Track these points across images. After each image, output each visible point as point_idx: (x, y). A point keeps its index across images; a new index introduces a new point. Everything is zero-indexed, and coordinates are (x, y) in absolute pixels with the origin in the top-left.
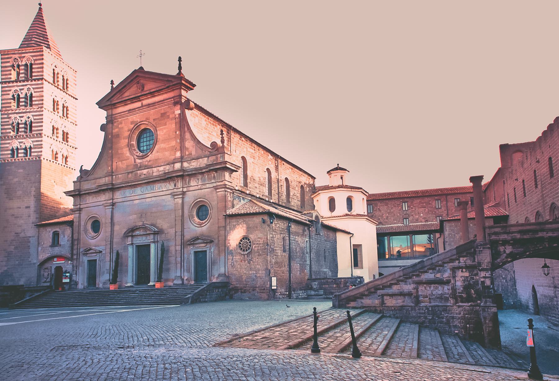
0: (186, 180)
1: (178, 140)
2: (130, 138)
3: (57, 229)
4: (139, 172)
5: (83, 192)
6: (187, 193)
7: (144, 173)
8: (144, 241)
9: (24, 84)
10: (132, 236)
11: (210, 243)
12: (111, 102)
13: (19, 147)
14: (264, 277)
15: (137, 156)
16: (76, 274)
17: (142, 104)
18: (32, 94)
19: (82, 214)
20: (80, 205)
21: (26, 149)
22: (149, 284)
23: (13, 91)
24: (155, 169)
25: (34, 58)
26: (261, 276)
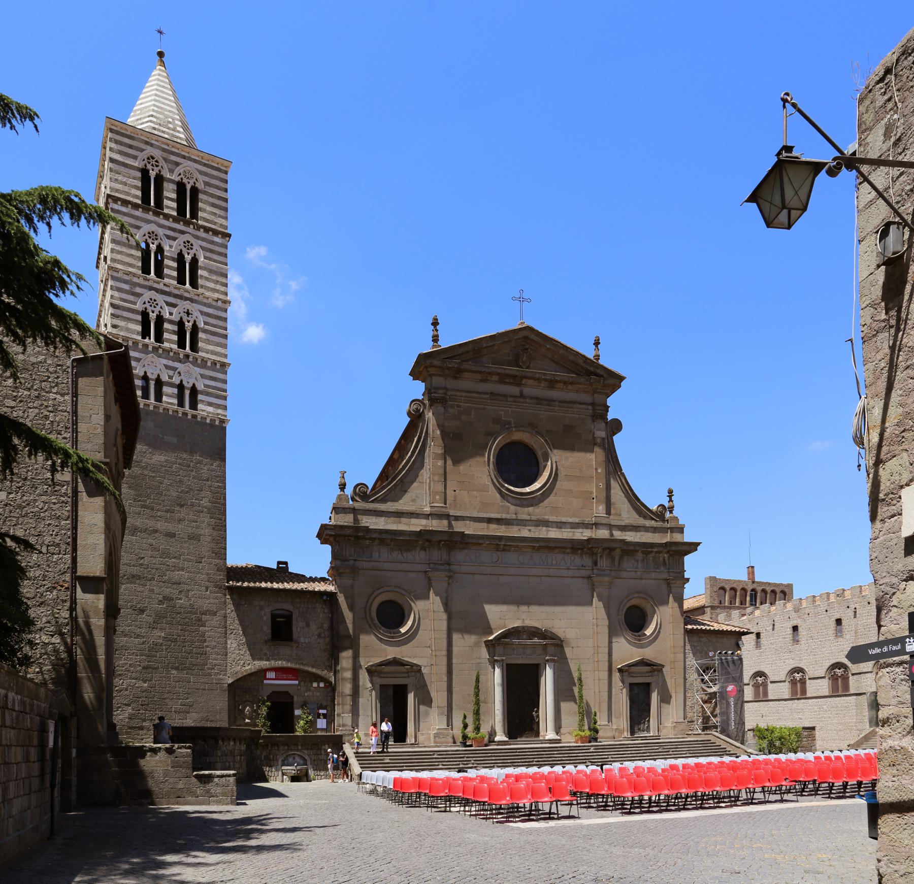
20: (355, 560)
21: (181, 387)
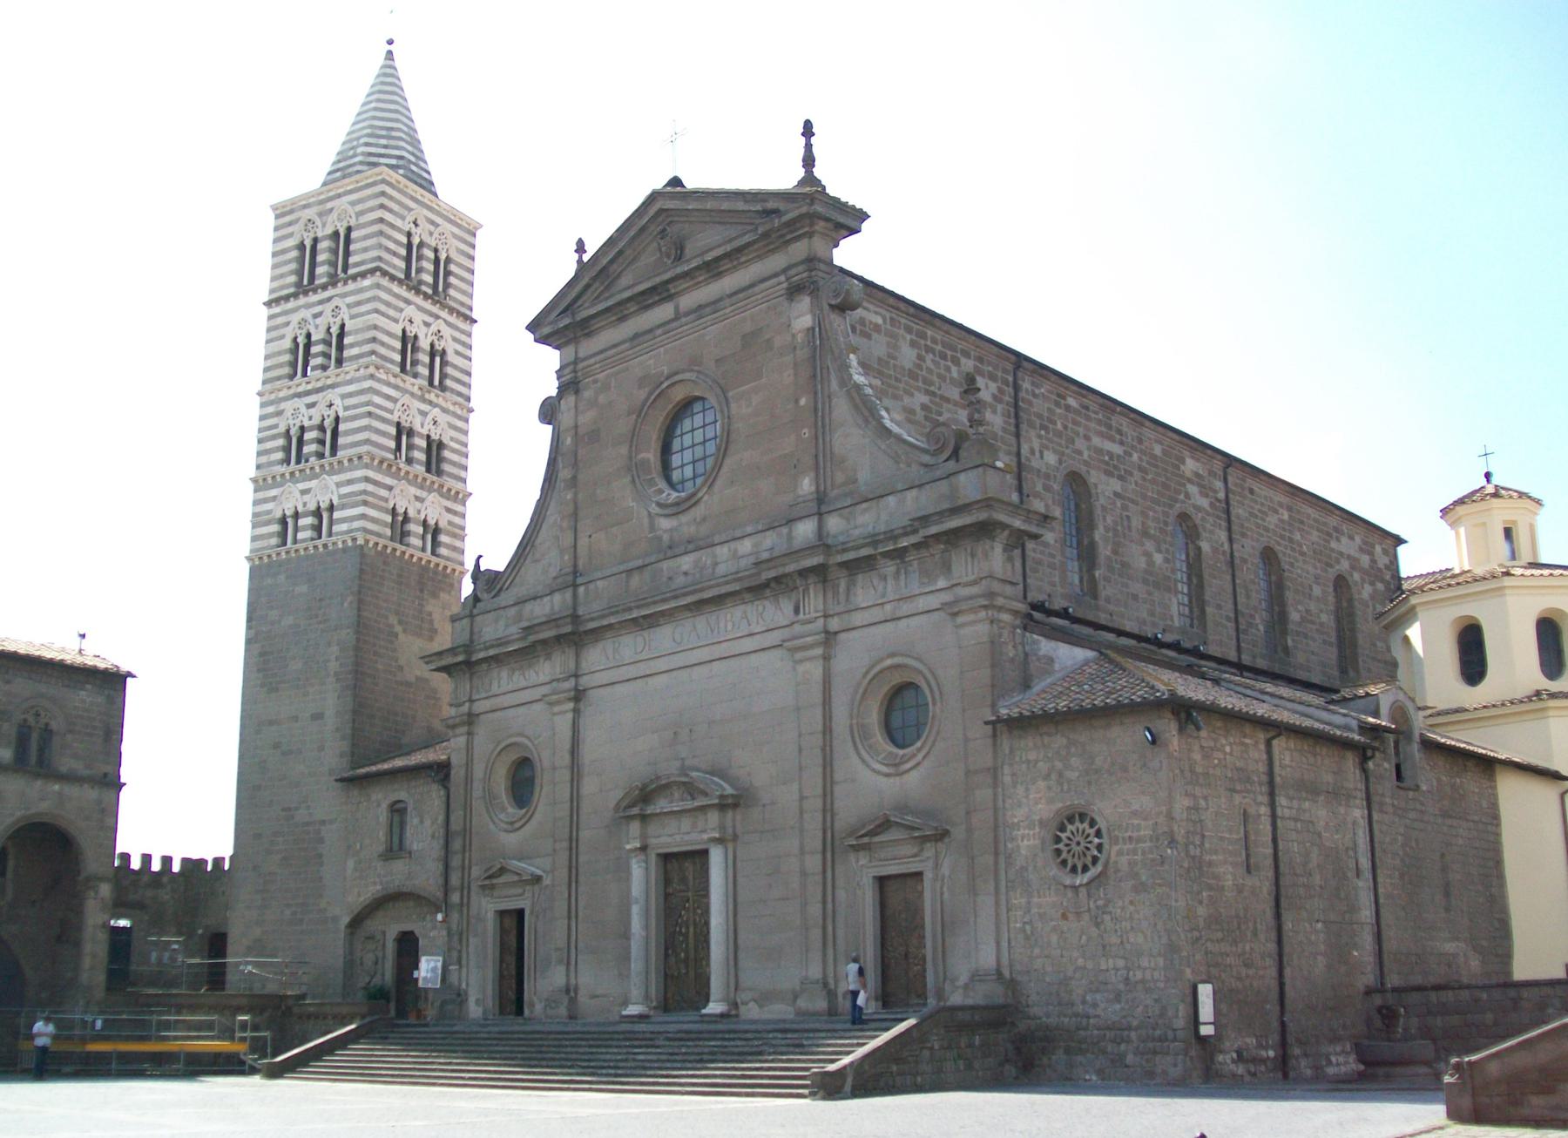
0: (838, 586)
1: (806, 430)
2: (633, 438)
3: (401, 793)
4: (665, 565)
5: (482, 655)
6: (842, 636)
7: (685, 568)
8: (686, 838)
9: (326, 294)
10: (644, 818)
11: (936, 841)
12: (573, 314)
13: (300, 509)
14: (1161, 985)
15: (659, 505)
16: (459, 962)
17: (677, 308)
18: (343, 326)
19: (476, 737)
20: (471, 701)
21: (317, 513)
22: (704, 1011)
23: (294, 324)
24: (723, 552)
25: (359, 208)
26: (1148, 977)
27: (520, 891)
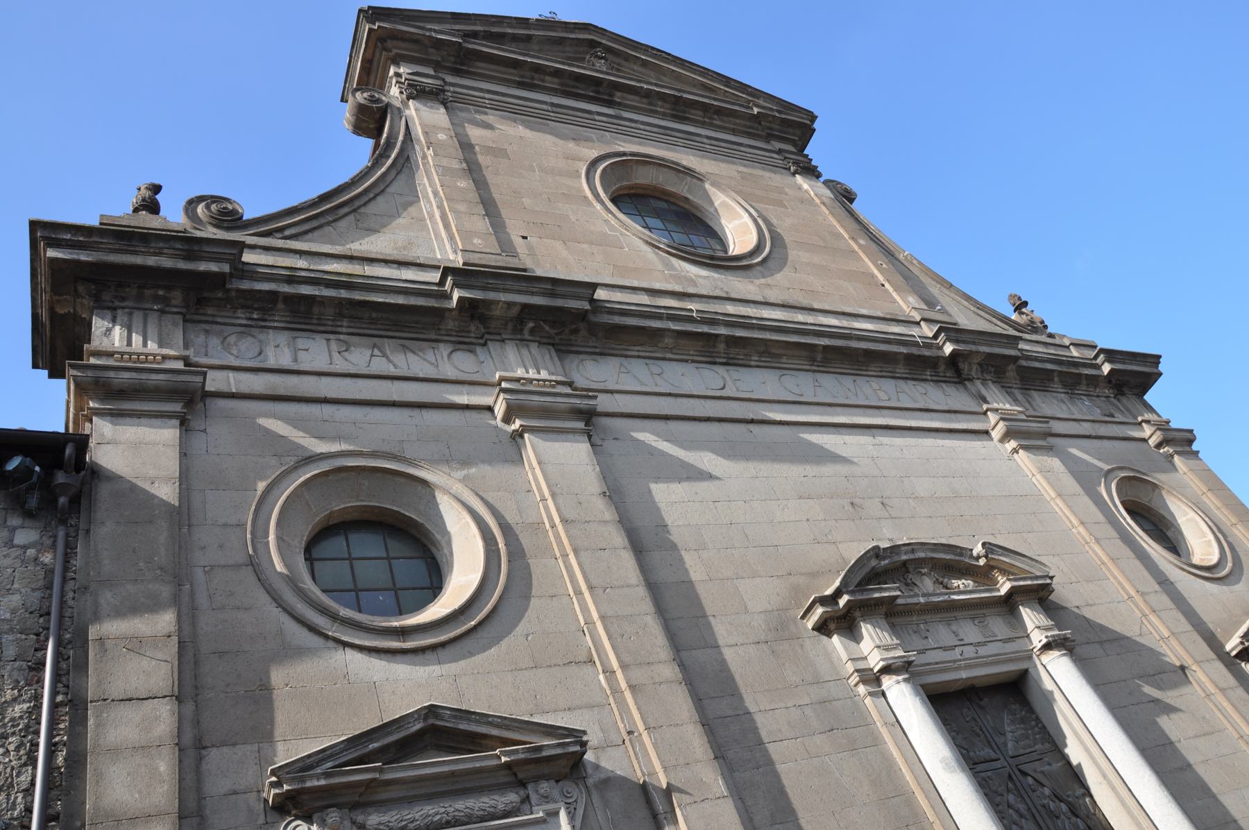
27: (512, 797)
